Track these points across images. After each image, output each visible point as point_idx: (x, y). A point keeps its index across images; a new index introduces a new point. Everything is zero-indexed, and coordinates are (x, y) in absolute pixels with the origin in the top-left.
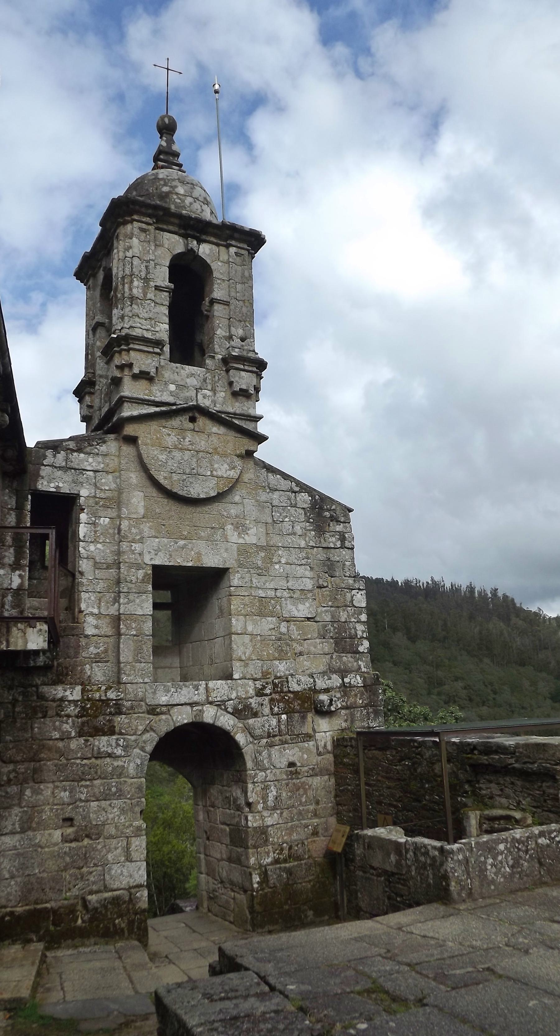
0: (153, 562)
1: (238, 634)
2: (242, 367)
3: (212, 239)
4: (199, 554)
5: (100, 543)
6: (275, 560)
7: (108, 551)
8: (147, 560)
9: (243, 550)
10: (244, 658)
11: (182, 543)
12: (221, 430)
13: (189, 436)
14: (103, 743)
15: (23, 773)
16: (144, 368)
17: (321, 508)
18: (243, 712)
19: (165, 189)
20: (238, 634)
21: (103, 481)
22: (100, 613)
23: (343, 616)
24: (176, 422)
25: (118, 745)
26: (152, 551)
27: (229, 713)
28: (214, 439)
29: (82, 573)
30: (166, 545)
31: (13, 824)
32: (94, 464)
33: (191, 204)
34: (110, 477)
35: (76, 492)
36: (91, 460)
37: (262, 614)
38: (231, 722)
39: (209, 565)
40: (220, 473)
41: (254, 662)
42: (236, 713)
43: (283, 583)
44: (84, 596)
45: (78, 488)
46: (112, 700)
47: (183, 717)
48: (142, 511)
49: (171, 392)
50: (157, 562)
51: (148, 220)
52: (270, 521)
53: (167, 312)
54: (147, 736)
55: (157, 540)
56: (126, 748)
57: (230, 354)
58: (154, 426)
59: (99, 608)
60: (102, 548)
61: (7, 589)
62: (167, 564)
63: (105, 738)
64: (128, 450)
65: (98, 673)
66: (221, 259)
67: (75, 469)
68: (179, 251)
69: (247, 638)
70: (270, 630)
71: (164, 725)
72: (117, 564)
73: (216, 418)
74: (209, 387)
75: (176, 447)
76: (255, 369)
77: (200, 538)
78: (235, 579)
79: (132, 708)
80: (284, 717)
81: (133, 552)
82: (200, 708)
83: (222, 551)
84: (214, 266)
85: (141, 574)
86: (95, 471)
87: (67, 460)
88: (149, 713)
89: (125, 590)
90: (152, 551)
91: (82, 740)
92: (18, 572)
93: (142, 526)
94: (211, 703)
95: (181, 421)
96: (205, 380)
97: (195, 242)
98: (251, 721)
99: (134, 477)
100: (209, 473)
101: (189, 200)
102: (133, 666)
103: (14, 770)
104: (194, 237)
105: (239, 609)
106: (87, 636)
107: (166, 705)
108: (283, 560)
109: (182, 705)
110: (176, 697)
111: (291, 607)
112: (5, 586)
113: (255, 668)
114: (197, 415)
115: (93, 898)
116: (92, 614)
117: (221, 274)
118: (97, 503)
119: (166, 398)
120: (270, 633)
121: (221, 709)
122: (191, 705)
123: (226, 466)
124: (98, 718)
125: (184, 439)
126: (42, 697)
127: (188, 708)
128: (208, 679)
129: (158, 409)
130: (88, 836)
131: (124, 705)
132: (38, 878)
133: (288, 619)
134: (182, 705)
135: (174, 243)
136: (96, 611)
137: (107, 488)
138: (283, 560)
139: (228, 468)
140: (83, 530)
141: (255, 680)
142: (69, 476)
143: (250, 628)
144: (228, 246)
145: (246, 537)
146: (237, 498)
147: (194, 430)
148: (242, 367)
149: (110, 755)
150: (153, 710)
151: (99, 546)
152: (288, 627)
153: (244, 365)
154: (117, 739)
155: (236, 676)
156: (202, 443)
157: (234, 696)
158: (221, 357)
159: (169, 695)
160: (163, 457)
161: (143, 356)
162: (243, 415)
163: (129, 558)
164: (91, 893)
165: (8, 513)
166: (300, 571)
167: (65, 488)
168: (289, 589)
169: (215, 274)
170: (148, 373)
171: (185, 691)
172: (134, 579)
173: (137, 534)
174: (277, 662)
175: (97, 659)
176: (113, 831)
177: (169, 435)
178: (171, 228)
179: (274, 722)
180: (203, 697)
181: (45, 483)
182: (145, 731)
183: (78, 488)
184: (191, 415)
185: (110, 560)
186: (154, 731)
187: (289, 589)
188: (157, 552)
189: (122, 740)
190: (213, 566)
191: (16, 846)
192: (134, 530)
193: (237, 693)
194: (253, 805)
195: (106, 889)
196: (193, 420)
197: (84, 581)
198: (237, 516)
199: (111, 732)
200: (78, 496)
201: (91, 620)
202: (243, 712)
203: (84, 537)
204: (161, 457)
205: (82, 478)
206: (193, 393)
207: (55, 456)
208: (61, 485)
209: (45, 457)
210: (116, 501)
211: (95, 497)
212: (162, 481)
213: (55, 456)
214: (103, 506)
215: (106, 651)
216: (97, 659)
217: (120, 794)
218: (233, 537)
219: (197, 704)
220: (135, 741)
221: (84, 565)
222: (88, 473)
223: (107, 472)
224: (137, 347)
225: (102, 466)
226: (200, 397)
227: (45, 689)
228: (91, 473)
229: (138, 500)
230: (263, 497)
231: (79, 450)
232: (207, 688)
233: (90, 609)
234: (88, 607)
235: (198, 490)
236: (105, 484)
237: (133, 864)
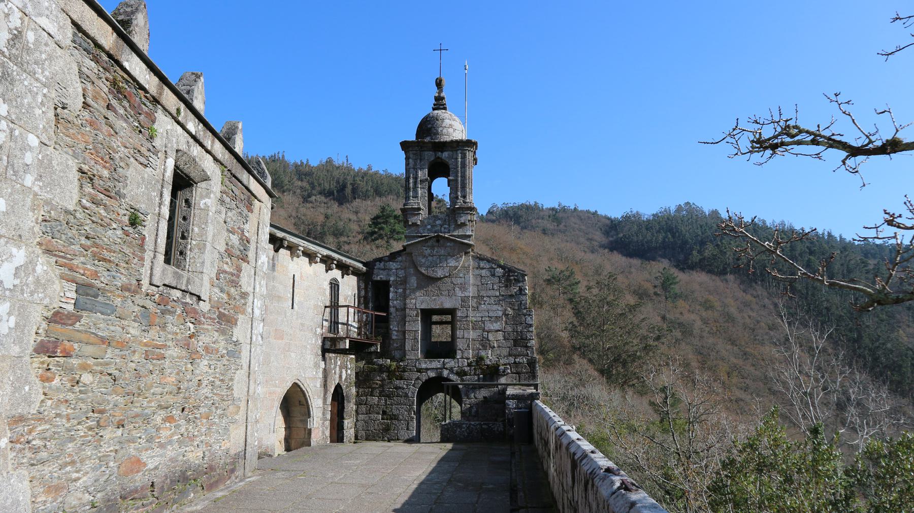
9: (464, 300)
13: (436, 249)
17: (509, 276)
19: (429, 126)
23: (519, 329)
24: (430, 243)
28: (448, 249)
42: (457, 374)
48: (415, 285)
71: (424, 377)
72: (404, 309)
78: (459, 314)
84: (450, 162)
99: (412, 271)
122: (437, 369)
135: (429, 156)
140: (391, 295)
142: (385, 273)
149: (400, 388)
150: (419, 371)
160: (423, 260)
166: (495, 307)
175: (397, 349)
179: (476, 378)
196: (438, 241)
201: (395, 333)
202: (461, 373)
205: (391, 273)
210: (404, 282)
216: (397, 349)
218: (459, 293)
221: (392, 310)
229: (413, 281)
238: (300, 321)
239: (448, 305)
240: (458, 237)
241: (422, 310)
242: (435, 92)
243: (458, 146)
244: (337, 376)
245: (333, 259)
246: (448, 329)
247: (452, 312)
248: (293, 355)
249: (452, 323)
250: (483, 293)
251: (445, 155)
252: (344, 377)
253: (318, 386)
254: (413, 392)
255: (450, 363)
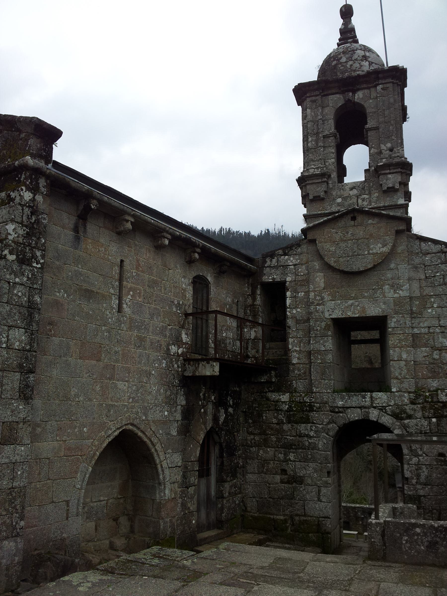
0: (331, 317)
1: (395, 361)
2: (388, 171)
3: (365, 86)
4: (364, 308)
5: (299, 308)
6: (428, 305)
7: (304, 312)
8: (327, 315)
9: (398, 302)
10: (400, 377)
11: (350, 302)
12: (376, 220)
14: (302, 428)
15: (258, 441)
16: (316, 194)
18: (398, 415)
20: (395, 361)
21: (300, 270)
22: (300, 350)
24: (341, 223)
25: (312, 430)
26: (330, 310)
27: (389, 415)
29: (289, 327)
30: (339, 305)
31: (254, 468)
32: (294, 261)
33: (351, 65)
34: (304, 267)
35: (284, 280)
36: (292, 259)
37: (414, 346)
38: (390, 421)
39: (371, 315)
40: (375, 251)
41: (408, 380)
43: (435, 322)
44: (291, 340)
45: (285, 277)
46: (307, 402)
47: (355, 415)
48: (322, 285)
49: (338, 203)
50: (333, 316)
51: (317, 93)
52: (423, 277)
53: (333, 151)
54: (331, 426)
55: (333, 302)
56: (316, 432)
57: (377, 166)
58: (327, 230)
59: (300, 347)
60: (300, 311)
61: (249, 339)
62: (341, 316)
63: (303, 425)
64: (311, 248)
65: (300, 385)
66: (372, 97)
67: (283, 266)
68: (341, 104)
69: (403, 363)
70: (424, 357)
72: (308, 320)
73: (370, 214)
74: (367, 192)
75: (342, 240)
76: (400, 170)
77: (364, 297)
78: (392, 323)
79: (320, 408)
80: (434, 420)
81: (317, 311)
82: (367, 410)
83: (381, 304)
84: (366, 105)
85: (323, 324)
86: (295, 265)
87: (278, 261)
88: (332, 411)
89: (313, 336)
90: (330, 310)
91: (290, 425)
92: (254, 330)
93: (323, 295)
94: (375, 407)
95: (347, 221)
96: (363, 189)
97: (351, 94)
98: (406, 421)
99: (317, 265)
100: (366, 252)
101: (351, 63)
102: (320, 382)
103: (254, 439)
104: (349, 91)
105: (395, 344)
106: (294, 364)
107: (343, 408)
108: (435, 306)
109: (354, 408)
110: (349, 403)
111: (443, 340)
112: (248, 338)
113: (409, 384)
114: (356, 214)
115: (297, 518)
116: (296, 351)
117: (372, 108)
118: (296, 284)
119: (334, 209)
120: (424, 359)
121: (383, 412)
123: (380, 245)
124: (301, 413)
125: (347, 233)
126: (268, 399)
127: (359, 410)
128: (372, 392)
129: (325, 219)
130: (295, 482)
131: (314, 406)
132: (267, 500)
133: (440, 348)
134: (354, 408)
135: (336, 100)
136: (298, 349)
137: (302, 274)
138: (435, 306)
139: (381, 246)
140: (288, 301)
141: (410, 392)
143: (404, 356)
144: (375, 86)
145: (401, 292)
146: (392, 266)
147: (354, 225)
148: (388, 171)
150: (333, 410)
151: (299, 310)
152: (440, 354)
153: (390, 169)
154: (311, 426)
155: (394, 390)
156: (360, 232)
157: (392, 403)
158: (373, 168)
159: (344, 401)
161: (315, 186)
162: (391, 206)
163: (315, 316)
164: (297, 515)
165: (248, 298)
167: (278, 278)
168: (441, 326)
169: (368, 110)
170: (319, 196)
171: (355, 398)
172: (319, 328)
173: (319, 300)
174: (430, 380)
176: (309, 481)
177: (337, 233)
178: (334, 91)
179: (426, 423)
180: (368, 404)
181: (266, 277)
182: (328, 423)
183: (285, 277)
184: (352, 215)
185: (305, 318)
186: (335, 423)
187: (441, 326)
188: (333, 310)
189: (314, 427)
190: (375, 315)
191: (255, 481)
192: (318, 298)
193: (395, 401)
194: (409, 480)
195: (305, 515)
196: (354, 219)
197: (290, 331)
198: (392, 279)
199: (307, 421)
200: (285, 282)
203: (289, 305)
204: (331, 249)
206: (355, 200)
207: (271, 261)
208: (275, 277)
209: (266, 262)
211: (295, 281)
212: (332, 264)
213: (271, 261)
214: (301, 285)
215: (305, 373)
217: (314, 460)
218: (390, 294)
219: (365, 407)
220: (322, 428)
222: (290, 267)
223: (302, 264)
224: (310, 182)
225: (299, 261)
226: (360, 201)
227: (269, 395)
228: (292, 267)
229: (320, 279)
230: (417, 260)
231: (285, 254)
232: (371, 397)
233: (295, 348)
234: (293, 347)
235: (359, 265)
236: (301, 271)
237: (322, 503)
238: (135, 333)
239: (373, 310)
240: (385, 208)
241: (334, 320)
242: (340, 22)
243: (378, 78)
244: (209, 418)
245: (194, 245)
246: (375, 349)
247: (379, 323)
248: (121, 385)
249: (382, 342)
250: (428, 291)
251: (359, 96)
252: (222, 418)
253: (174, 432)
254: (323, 443)
255: (381, 397)
